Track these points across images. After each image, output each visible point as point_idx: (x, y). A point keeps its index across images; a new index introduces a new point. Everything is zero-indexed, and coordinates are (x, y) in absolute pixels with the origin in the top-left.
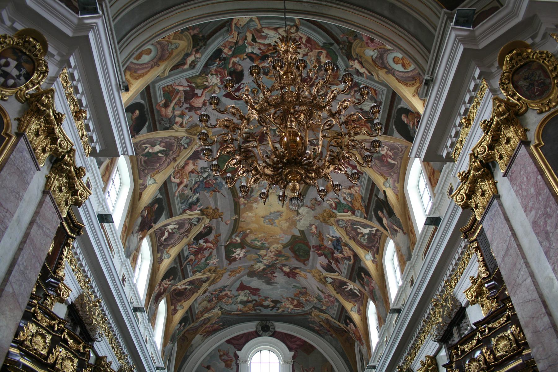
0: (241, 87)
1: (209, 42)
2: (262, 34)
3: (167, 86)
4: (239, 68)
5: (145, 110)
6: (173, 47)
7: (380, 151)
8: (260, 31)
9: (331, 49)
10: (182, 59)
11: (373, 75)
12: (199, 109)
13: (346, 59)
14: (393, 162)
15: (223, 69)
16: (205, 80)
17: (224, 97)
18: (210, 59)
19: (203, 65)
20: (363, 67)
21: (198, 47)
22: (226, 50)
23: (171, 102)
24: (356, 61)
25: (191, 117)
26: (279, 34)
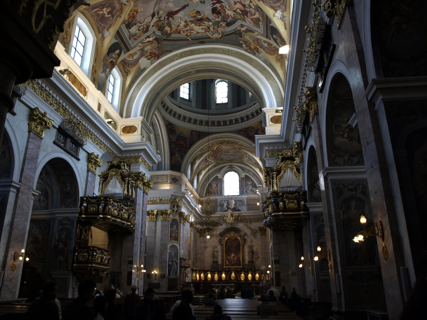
0: (212, 5)
1: (234, 31)
2: (205, 30)
3: (257, 27)
4: (215, 15)
5: (270, 31)
6: (252, 38)
7: (107, 9)
8: (206, 31)
9: (166, 35)
10: (248, 32)
11: (142, 43)
12: (238, 2)
13: (157, 37)
14: (95, 10)
15: (225, 17)
16: (235, 16)
17: (223, 1)
18: (232, 24)
19: (236, 23)
20: (148, 42)
21: (239, 32)
22: (224, 25)
23: (256, 18)
24: (152, 40)
25: (244, 1)
26: (196, 31)
